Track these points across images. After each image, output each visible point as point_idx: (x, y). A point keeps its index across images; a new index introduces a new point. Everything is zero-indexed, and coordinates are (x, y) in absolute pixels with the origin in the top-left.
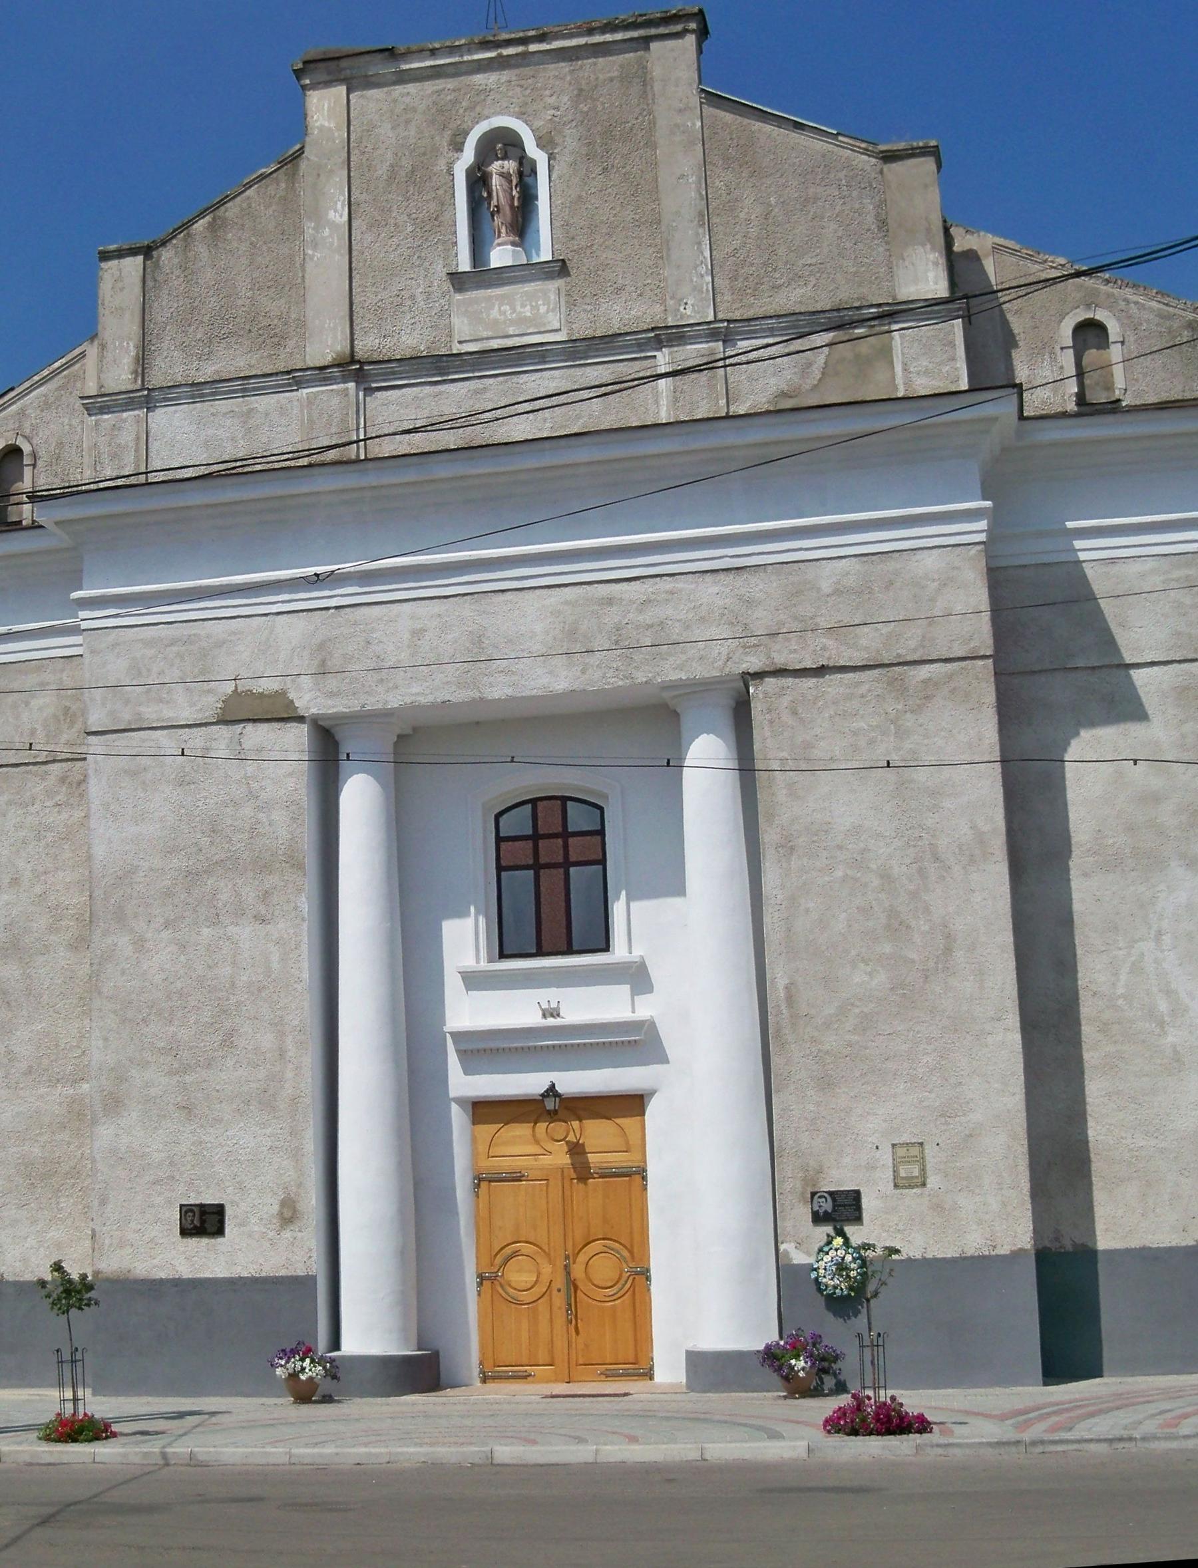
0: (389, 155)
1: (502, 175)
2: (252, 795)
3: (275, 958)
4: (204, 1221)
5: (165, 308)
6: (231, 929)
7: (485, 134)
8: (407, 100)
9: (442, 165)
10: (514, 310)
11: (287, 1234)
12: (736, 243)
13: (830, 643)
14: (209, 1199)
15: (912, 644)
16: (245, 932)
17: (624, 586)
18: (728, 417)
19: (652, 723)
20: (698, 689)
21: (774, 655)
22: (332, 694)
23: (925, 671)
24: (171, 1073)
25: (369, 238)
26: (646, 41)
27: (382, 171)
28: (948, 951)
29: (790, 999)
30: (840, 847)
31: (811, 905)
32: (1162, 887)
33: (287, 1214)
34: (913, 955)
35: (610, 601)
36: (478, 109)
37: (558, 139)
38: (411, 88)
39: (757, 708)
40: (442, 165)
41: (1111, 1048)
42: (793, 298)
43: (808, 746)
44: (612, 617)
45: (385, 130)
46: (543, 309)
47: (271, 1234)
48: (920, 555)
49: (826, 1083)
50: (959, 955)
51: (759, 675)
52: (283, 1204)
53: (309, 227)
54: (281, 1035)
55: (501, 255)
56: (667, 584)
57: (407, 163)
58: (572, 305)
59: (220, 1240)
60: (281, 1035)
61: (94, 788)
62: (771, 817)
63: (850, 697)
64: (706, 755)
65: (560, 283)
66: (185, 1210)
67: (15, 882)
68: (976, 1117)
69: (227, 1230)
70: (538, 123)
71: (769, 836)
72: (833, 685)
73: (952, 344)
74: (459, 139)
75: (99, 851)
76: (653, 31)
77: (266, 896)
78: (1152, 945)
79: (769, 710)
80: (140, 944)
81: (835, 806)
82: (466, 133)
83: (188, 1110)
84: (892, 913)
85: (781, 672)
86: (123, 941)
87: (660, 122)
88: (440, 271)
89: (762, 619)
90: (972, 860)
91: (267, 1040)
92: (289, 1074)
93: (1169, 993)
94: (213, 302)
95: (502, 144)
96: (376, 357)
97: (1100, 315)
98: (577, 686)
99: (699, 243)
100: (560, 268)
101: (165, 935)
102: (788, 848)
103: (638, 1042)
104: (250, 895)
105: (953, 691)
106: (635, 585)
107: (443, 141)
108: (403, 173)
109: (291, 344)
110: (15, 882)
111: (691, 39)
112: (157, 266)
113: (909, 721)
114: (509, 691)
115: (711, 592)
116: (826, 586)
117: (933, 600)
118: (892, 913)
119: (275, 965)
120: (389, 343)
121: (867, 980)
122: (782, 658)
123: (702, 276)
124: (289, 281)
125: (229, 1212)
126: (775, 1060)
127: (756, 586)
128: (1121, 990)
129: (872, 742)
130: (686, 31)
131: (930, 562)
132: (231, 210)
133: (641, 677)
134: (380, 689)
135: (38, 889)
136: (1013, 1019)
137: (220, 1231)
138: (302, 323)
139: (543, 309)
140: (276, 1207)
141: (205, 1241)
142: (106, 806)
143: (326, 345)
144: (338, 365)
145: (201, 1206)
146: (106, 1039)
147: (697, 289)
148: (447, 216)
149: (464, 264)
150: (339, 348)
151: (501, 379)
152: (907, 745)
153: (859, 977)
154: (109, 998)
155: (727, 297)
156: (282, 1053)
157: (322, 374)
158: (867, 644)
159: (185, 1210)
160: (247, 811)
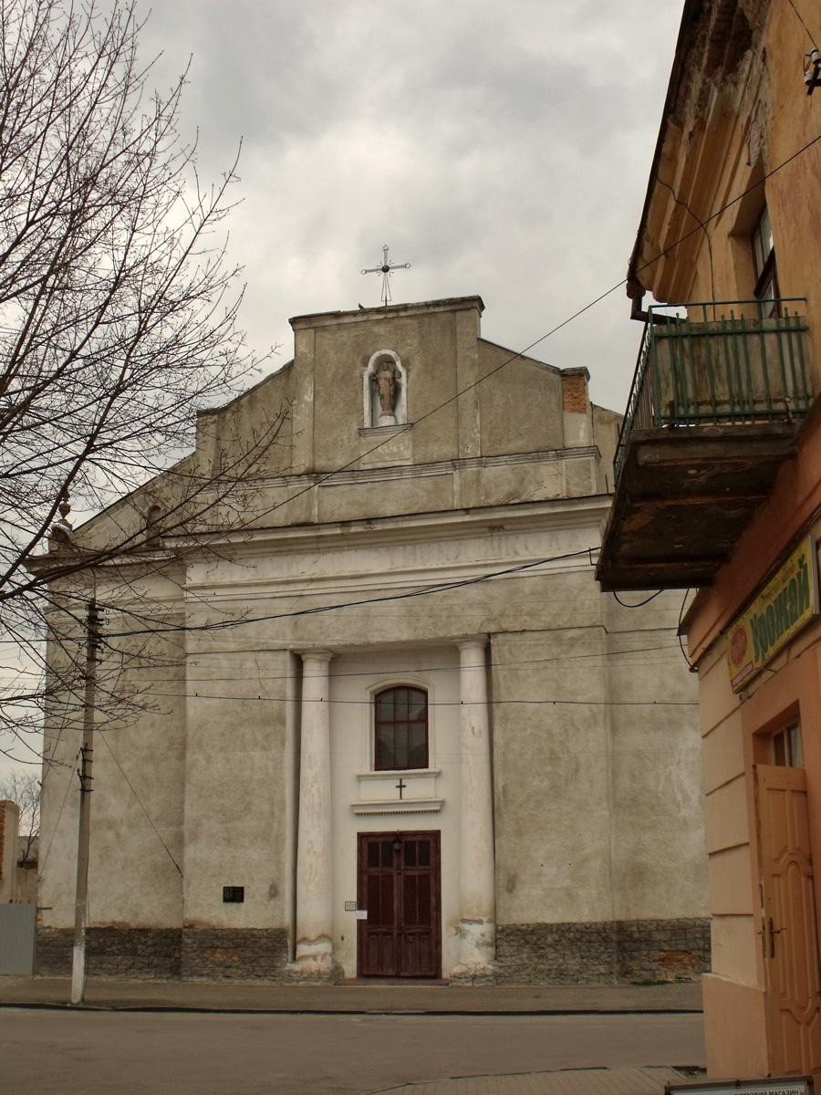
0: (333, 368)
1: (385, 379)
4: (234, 895)
6: (252, 753)
7: (378, 358)
8: (342, 339)
9: (357, 373)
10: (388, 448)
11: (272, 902)
12: (492, 418)
13: (527, 618)
15: (566, 620)
16: (257, 755)
19: (447, 652)
21: (502, 624)
23: (571, 633)
24: (222, 823)
25: (323, 409)
26: (454, 311)
27: (329, 375)
29: (504, 792)
30: (529, 719)
31: (515, 747)
32: (681, 739)
33: (273, 892)
34: (561, 772)
36: (375, 345)
37: (411, 362)
38: (345, 334)
39: (494, 650)
40: (357, 373)
41: (654, 818)
42: (516, 445)
45: (332, 354)
46: (402, 448)
47: (266, 902)
48: (572, 576)
54: (272, 805)
58: (415, 446)
59: (242, 904)
60: (272, 805)
63: (536, 645)
65: (410, 435)
66: (226, 889)
68: (587, 851)
69: (245, 900)
70: (402, 354)
74: (366, 360)
75: (191, 712)
76: (457, 307)
77: (266, 737)
78: (675, 767)
79: (499, 651)
80: (208, 759)
81: (528, 690)
82: (370, 358)
83: (228, 840)
84: (553, 752)
85: (505, 632)
86: (201, 757)
87: (459, 354)
88: (355, 427)
91: (266, 807)
92: (276, 825)
95: (386, 362)
96: (325, 470)
98: (412, 638)
99: (475, 417)
100: (411, 426)
104: (259, 736)
108: (339, 376)
114: (380, 639)
116: (527, 590)
119: (271, 771)
122: (505, 626)
123: (475, 433)
125: (246, 891)
126: (497, 822)
128: (660, 789)
133: (441, 635)
134: (322, 637)
137: (242, 901)
139: (402, 448)
140: (268, 890)
141: (235, 905)
144: (307, 474)
145: (233, 887)
146: (191, 805)
147: (473, 440)
149: (367, 424)
150: (307, 465)
151: (382, 483)
154: (194, 785)
155: (488, 444)
156: (272, 814)
158: (546, 619)
159: (226, 889)
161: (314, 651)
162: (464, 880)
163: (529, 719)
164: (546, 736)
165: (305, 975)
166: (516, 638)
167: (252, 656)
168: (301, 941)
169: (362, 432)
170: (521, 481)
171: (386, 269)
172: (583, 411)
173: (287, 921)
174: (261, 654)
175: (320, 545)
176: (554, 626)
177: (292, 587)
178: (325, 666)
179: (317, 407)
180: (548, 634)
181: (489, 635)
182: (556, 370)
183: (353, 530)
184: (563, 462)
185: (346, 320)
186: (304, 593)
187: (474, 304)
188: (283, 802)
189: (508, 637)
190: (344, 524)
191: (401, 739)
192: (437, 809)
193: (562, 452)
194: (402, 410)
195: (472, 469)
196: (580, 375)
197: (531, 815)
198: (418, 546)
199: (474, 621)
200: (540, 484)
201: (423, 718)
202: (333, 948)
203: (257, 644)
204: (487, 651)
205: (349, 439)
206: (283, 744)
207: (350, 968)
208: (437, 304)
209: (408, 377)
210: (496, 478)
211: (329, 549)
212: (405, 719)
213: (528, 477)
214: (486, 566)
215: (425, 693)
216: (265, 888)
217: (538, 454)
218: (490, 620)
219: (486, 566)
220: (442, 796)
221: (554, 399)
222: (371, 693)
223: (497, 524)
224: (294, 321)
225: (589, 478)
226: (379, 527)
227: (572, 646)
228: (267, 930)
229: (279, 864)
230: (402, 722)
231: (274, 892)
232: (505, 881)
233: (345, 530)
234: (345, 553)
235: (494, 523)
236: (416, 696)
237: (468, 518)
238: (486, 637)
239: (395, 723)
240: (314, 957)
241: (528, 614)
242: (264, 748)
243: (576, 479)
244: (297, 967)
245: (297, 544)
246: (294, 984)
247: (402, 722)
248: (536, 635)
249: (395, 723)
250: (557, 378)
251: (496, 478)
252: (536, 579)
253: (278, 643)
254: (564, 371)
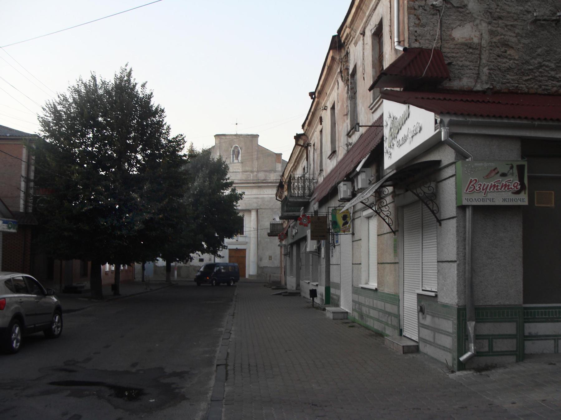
19: (249, 211)
20: (253, 209)
64: (254, 214)
100: (242, 163)
115: (255, 200)
122: (261, 207)
127: (259, 200)
166: (264, 210)
172: (280, 163)
192: (246, 243)
193: (275, 171)
194: (240, 158)
195: (255, 173)
196: (280, 155)
199: (255, 206)
217: (270, 171)
220: (247, 241)
232: (260, 259)
250: (275, 156)
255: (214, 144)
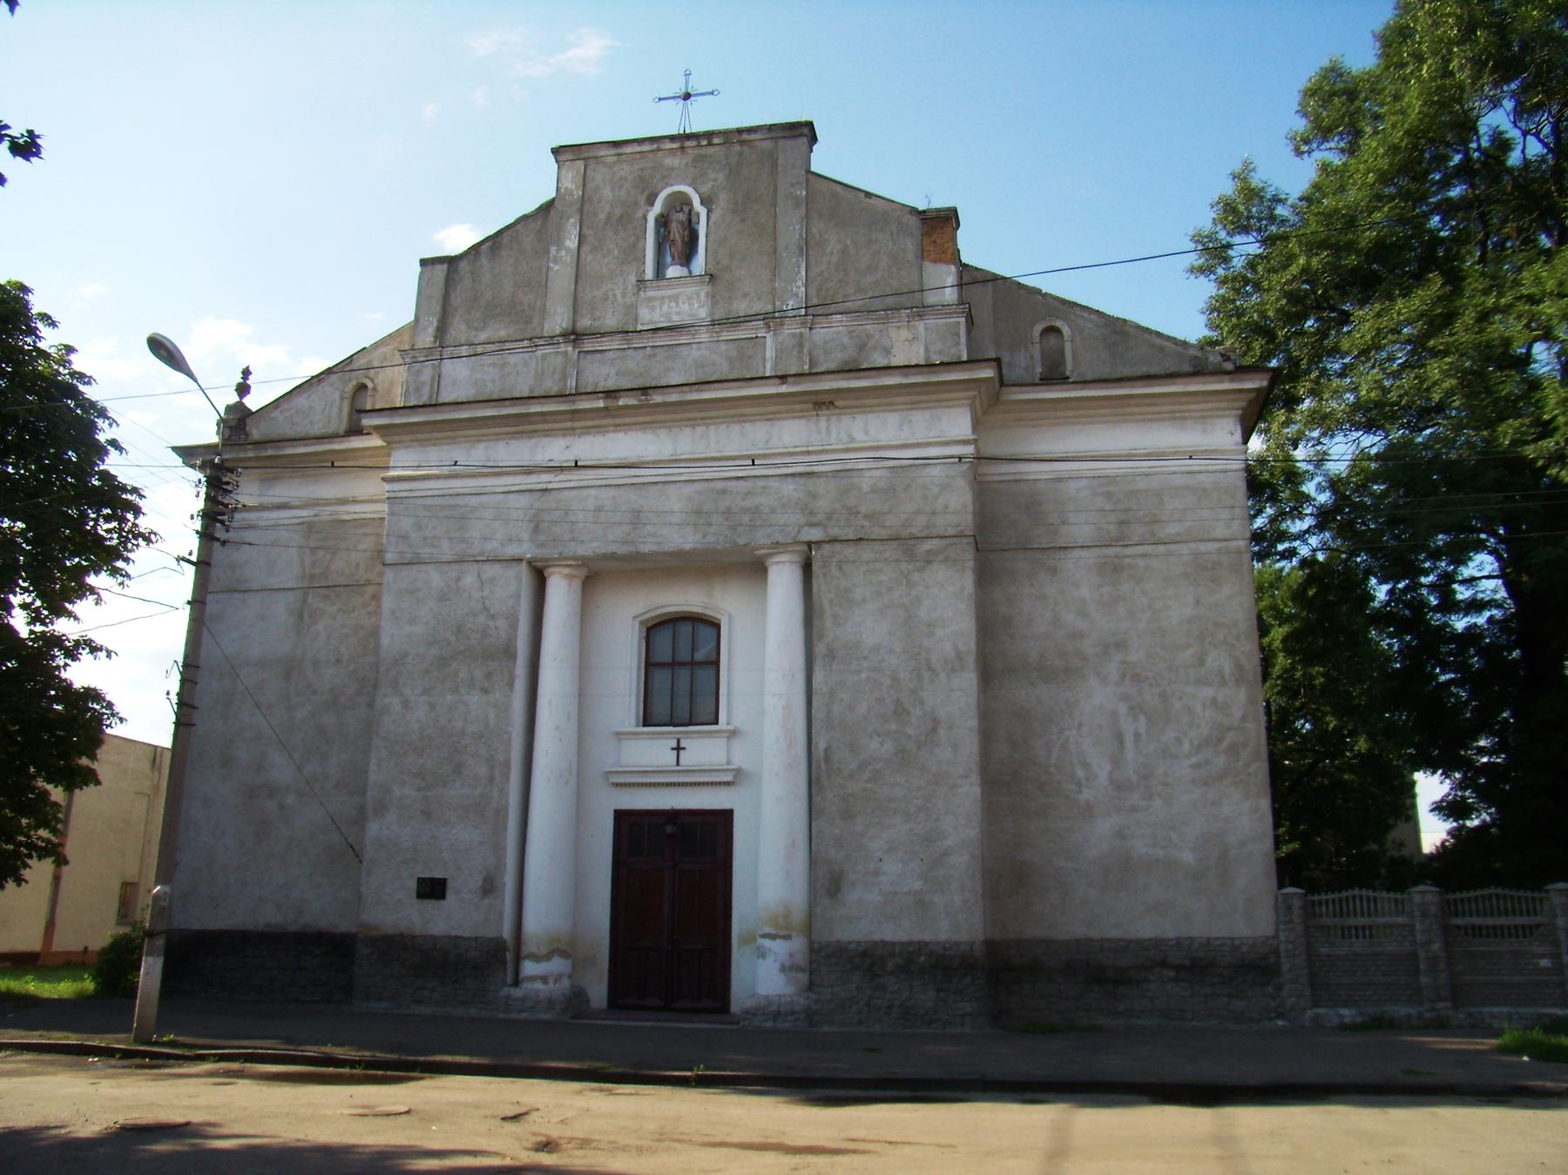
0: (607, 208)
2: (486, 609)
3: (492, 716)
4: (433, 889)
5: (458, 298)
9: (640, 214)
11: (486, 901)
13: (866, 523)
14: (437, 875)
16: (474, 699)
17: (734, 483)
18: (810, 374)
22: (542, 545)
23: (927, 546)
24: (419, 790)
25: (590, 258)
27: (602, 216)
28: (934, 730)
29: (827, 758)
30: (865, 658)
34: (910, 731)
35: (724, 492)
40: (640, 214)
43: (847, 590)
44: (724, 504)
45: (607, 193)
49: (848, 815)
50: (942, 732)
51: (818, 543)
52: (485, 880)
53: (553, 250)
55: (673, 271)
56: (760, 483)
57: (618, 212)
58: (714, 304)
61: (387, 602)
62: (821, 637)
66: (421, 881)
67: (338, 661)
68: (949, 842)
71: (820, 649)
72: (867, 552)
73: (958, 335)
77: (488, 676)
80: (406, 704)
82: (656, 195)
83: (428, 814)
84: (898, 702)
86: (395, 702)
88: (633, 279)
89: (823, 505)
90: (953, 670)
91: (483, 771)
93: (1086, 765)
94: (488, 295)
95: (681, 202)
97: (1059, 324)
100: (711, 277)
101: (422, 698)
102: (831, 656)
103: (736, 778)
104: (478, 674)
105: (946, 559)
106: (742, 483)
107: (642, 200)
109: (535, 321)
110: (338, 661)
111: (805, 140)
112: (456, 271)
113: (916, 577)
114: (654, 548)
115: (790, 489)
116: (866, 489)
117: (936, 498)
118: (898, 702)
119: (492, 722)
120: (596, 324)
121: (877, 747)
122: (835, 532)
124: (540, 285)
125: (450, 885)
126: (816, 799)
127: (820, 485)
129: (890, 589)
130: (801, 135)
131: (936, 471)
132: (506, 239)
133: (741, 541)
135: (352, 667)
136: (975, 778)
137: (442, 896)
138: (544, 309)
142: (393, 613)
143: (558, 320)
148: (640, 245)
149: (649, 273)
152: (914, 593)
153: (874, 745)
156: (491, 780)
157: (551, 340)
159: (421, 881)
160: (481, 619)
161: (561, 560)
162: (767, 873)
163: (865, 658)
164: (888, 682)
165: (529, 1004)
166: (849, 551)
167: (474, 568)
168: (526, 957)
169: (641, 282)
170: (862, 347)
171: (687, 96)
173: (507, 932)
174: (486, 566)
175: (577, 424)
176: (904, 534)
177: (533, 479)
178: (577, 584)
179: (583, 256)
180: (894, 544)
181: (809, 544)
182: (914, 211)
183: (621, 402)
184: (920, 326)
185: (629, 149)
186: (550, 486)
187: (804, 132)
188: (507, 764)
189: (837, 547)
190: (610, 394)
191: (681, 677)
194: (699, 263)
197: (865, 790)
198: (712, 428)
200: (887, 351)
201: (714, 658)
202: (574, 968)
203: (482, 554)
204: (807, 568)
205: (624, 295)
206: (511, 684)
207: (598, 992)
208: (750, 130)
209: (708, 218)
210: (826, 342)
211: (587, 430)
212: (689, 659)
213: (873, 341)
214: (809, 453)
215: (716, 626)
216: (477, 881)
218: (811, 525)
219: (809, 453)
221: (910, 245)
222: (641, 623)
223: (828, 398)
224: (556, 151)
225: (958, 344)
226: (657, 398)
227: (929, 562)
228: (476, 939)
229: (499, 849)
230: (683, 664)
231: (490, 887)
232: (826, 880)
233: (610, 403)
234: (610, 436)
235: (822, 398)
236: (705, 632)
237: (784, 389)
238: (806, 548)
239: (674, 664)
240: (544, 979)
241: (866, 517)
242: (485, 691)
243: (939, 346)
244: (517, 993)
245: (546, 422)
246: (513, 1016)
247: (683, 664)
248: (877, 546)
249: (674, 664)
250: (913, 222)
251: (826, 342)
252: (878, 473)
253: (512, 550)
254: (924, 212)
255: (550, 194)
